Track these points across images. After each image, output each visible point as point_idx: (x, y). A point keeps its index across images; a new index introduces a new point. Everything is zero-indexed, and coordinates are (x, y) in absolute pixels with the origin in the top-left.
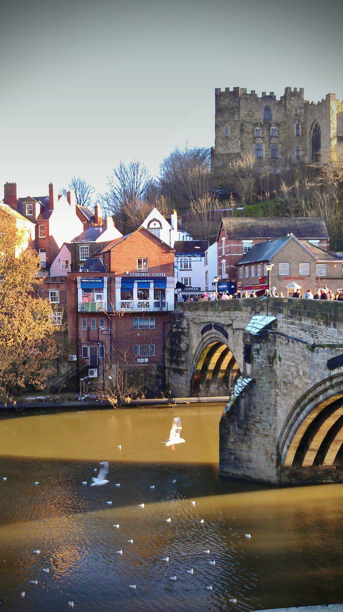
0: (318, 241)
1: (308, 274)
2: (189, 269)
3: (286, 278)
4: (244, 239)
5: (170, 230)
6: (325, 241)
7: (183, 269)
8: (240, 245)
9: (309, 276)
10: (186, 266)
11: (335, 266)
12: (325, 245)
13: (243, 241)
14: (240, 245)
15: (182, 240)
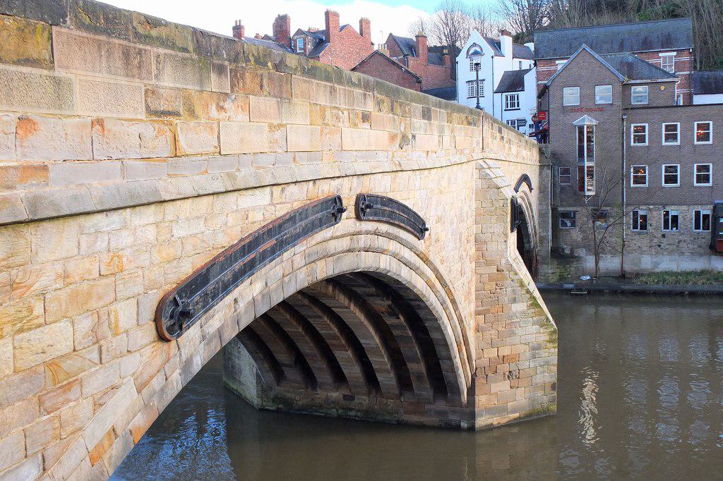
0: (675, 53)
1: (611, 102)
2: (516, 107)
3: (574, 109)
4: (557, 59)
5: (492, 57)
6: (686, 52)
7: (509, 108)
8: (553, 68)
9: (611, 105)
10: (513, 105)
11: (663, 88)
12: (686, 58)
13: (557, 62)
14: (553, 68)
15: (518, 69)
